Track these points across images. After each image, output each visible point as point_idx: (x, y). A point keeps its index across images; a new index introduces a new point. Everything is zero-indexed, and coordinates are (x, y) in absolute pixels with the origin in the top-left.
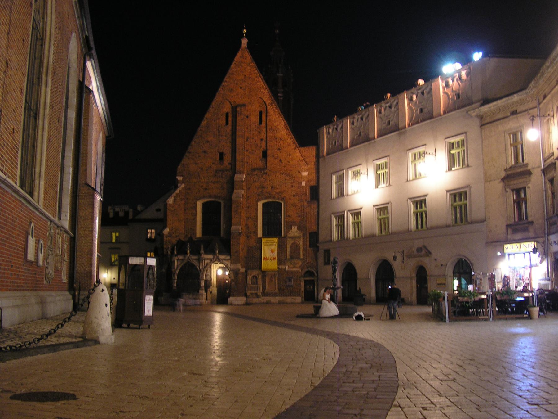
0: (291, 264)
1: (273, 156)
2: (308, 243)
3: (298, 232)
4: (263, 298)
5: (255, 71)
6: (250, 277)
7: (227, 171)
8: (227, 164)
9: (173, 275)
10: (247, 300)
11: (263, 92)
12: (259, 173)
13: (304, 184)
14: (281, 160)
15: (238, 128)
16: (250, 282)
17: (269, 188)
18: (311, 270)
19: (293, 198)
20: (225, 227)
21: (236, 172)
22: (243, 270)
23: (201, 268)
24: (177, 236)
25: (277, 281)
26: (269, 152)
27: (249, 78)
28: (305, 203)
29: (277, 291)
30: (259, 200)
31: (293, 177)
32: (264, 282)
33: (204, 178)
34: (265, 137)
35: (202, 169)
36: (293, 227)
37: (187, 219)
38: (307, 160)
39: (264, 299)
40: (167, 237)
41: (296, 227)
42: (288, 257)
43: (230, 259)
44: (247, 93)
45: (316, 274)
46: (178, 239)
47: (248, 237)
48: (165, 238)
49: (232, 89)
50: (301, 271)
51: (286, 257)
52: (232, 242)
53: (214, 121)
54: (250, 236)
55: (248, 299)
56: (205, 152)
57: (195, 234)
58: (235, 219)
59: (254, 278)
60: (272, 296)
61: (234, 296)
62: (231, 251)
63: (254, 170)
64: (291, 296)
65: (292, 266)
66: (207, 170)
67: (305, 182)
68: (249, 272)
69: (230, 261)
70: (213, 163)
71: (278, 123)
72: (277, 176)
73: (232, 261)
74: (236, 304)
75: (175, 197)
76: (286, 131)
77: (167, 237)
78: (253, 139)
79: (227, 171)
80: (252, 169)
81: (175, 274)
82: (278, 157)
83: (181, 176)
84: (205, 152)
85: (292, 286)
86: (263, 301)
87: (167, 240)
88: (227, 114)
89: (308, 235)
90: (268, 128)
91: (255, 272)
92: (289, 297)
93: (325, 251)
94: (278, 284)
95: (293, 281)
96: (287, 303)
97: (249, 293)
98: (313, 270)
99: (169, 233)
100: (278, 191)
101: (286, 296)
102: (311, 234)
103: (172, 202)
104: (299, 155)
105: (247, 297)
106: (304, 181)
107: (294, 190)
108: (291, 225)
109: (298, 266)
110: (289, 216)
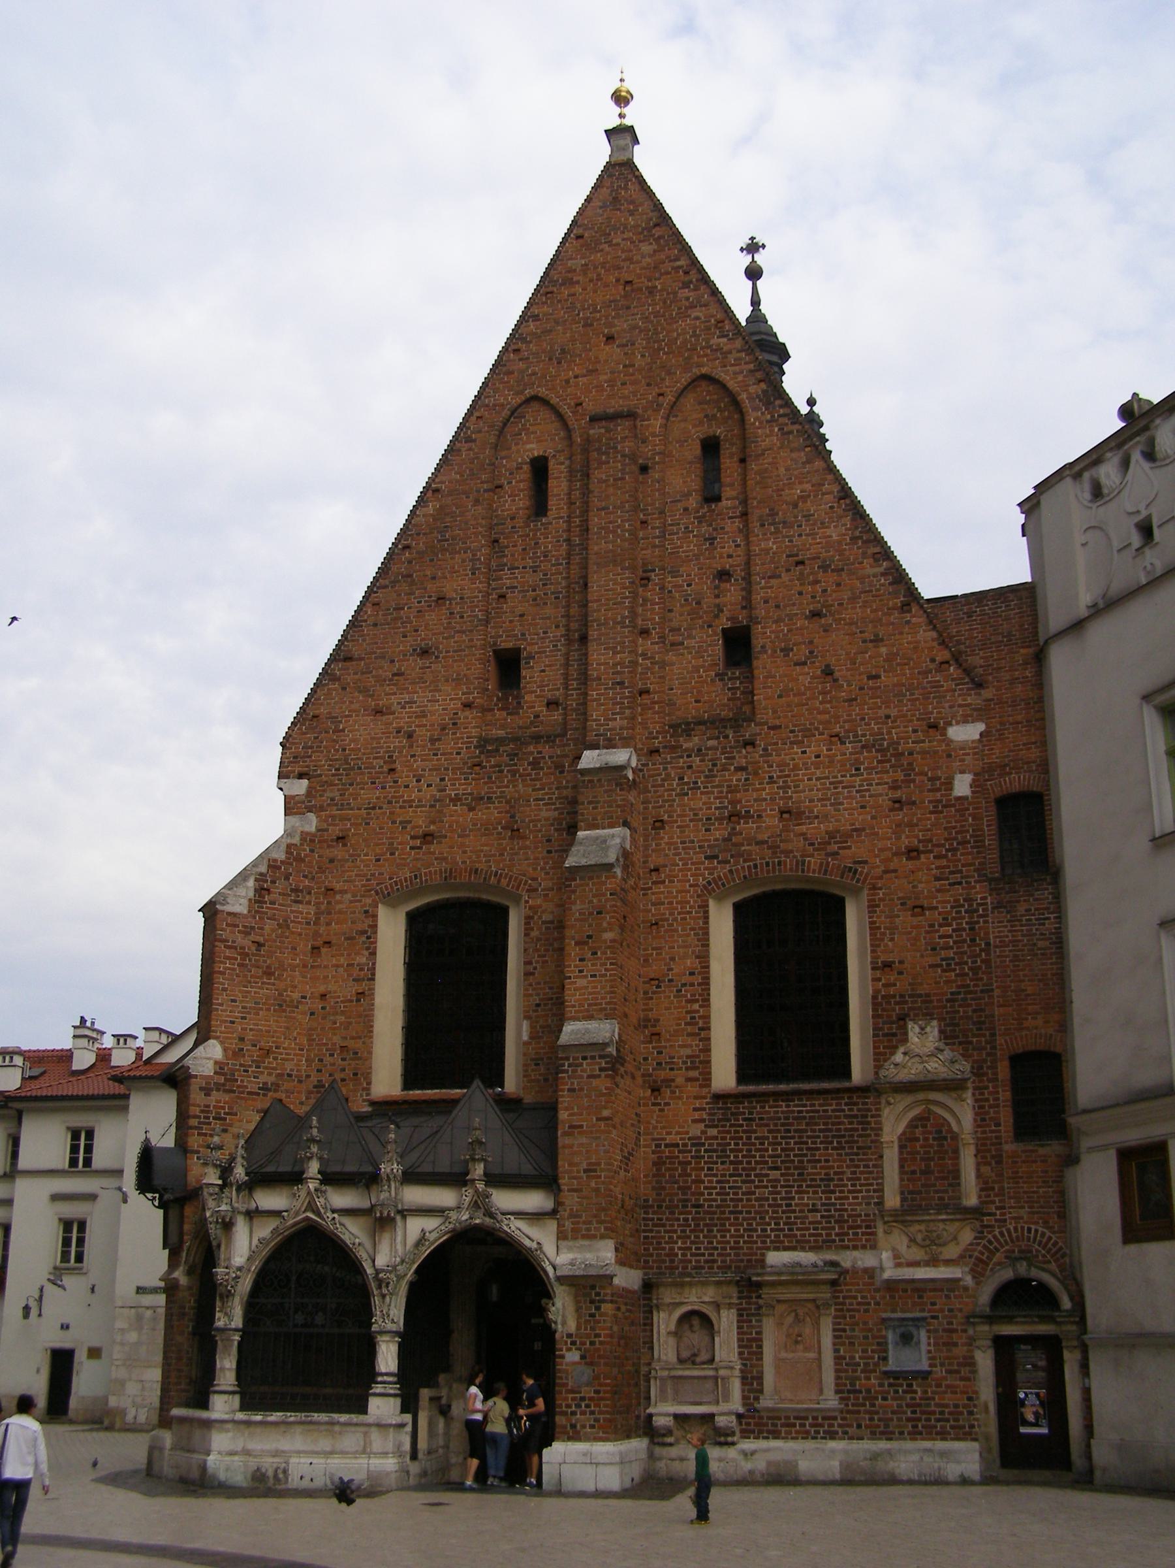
0: (912, 1240)
1: (786, 651)
2: (1006, 1117)
3: (948, 1054)
4: (748, 1445)
5: (677, 259)
6: (664, 1322)
7: (537, 738)
8: (540, 708)
9: (218, 1303)
10: (651, 1456)
11: (719, 349)
12: (711, 743)
13: (962, 786)
14: (828, 672)
15: (595, 521)
16: (666, 1349)
17: (772, 821)
18: (1034, 1273)
19: (911, 865)
20: (525, 1038)
21: (591, 737)
22: (628, 1279)
23: (381, 1261)
24: (265, 1088)
25: (827, 1340)
26: (761, 637)
27: (651, 291)
28: (980, 892)
29: (831, 1401)
30: (713, 890)
31: (899, 755)
32: (750, 1347)
33: (418, 781)
34: (740, 561)
35: (410, 736)
36: (913, 1029)
37: (323, 996)
38: (976, 660)
39: (753, 1453)
40: (207, 1091)
41: (933, 1030)
42: (892, 1200)
43: (553, 1213)
44: (639, 361)
45: (1066, 1304)
46: (263, 1103)
47: (655, 1090)
48: (197, 1097)
49: (563, 351)
50: (969, 1280)
51: (880, 1204)
52: (563, 1115)
53: (477, 502)
54: (668, 1082)
55: (658, 1450)
56: (425, 652)
57: (362, 1076)
58: (581, 982)
59: (696, 1322)
60: (806, 1436)
61: (574, 1435)
62: (563, 1165)
63: (685, 728)
64: (915, 1435)
65: (918, 1254)
66: (433, 741)
67: (968, 778)
68: (667, 1295)
69: (552, 1225)
70: (468, 705)
71: (808, 487)
72: (811, 750)
73: (568, 1225)
74: (590, 1487)
75: (261, 877)
76: (847, 521)
77: (207, 1091)
78: (675, 573)
79: (537, 738)
80: (674, 726)
81: (230, 1295)
82: (811, 652)
83: (301, 776)
84: (425, 652)
85: (924, 1375)
86: (747, 1466)
87: (206, 1110)
88: (539, 469)
89: (1003, 1070)
90: (755, 515)
91: (697, 1298)
92: (909, 1445)
93: (1126, 1156)
94: (838, 1359)
95: (924, 1347)
96: (893, 1480)
97: (663, 1411)
98: (1046, 1277)
99: (220, 1066)
100: (816, 829)
101: (888, 1435)
102: (1018, 1061)
103: (245, 902)
104: (926, 636)
105: (652, 1442)
106: (963, 772)
107: (911, 825)
108: (902, 1018)
109: (951, 1252)
110: (888, 965)
